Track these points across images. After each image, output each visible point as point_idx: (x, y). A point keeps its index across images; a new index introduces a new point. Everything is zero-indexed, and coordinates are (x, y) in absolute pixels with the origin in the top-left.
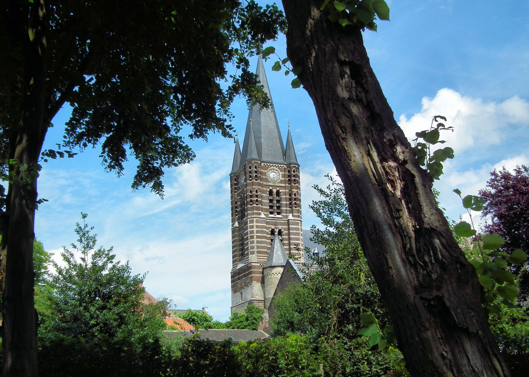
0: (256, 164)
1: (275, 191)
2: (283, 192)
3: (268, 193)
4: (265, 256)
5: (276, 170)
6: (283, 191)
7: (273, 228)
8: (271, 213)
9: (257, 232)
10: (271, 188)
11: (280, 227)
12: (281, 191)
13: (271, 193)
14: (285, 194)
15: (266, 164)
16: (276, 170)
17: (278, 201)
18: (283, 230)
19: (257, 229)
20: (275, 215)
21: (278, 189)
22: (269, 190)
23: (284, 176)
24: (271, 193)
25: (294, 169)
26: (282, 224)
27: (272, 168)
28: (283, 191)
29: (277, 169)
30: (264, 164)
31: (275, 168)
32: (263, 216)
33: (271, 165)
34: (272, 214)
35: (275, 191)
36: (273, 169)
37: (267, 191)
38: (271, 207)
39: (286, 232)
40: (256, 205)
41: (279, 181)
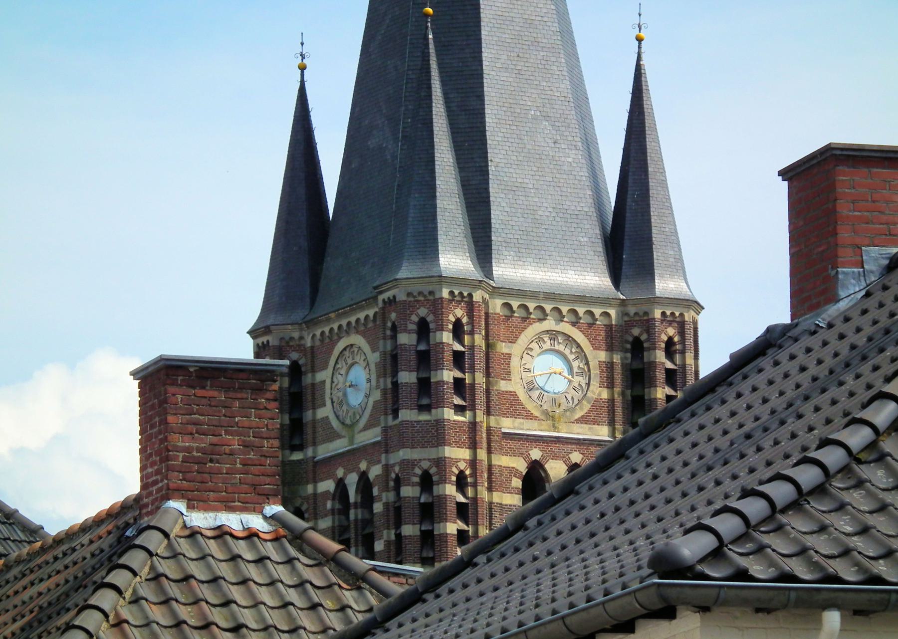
5: (568, 338)
22: (522, 466)
36: (553, 335)
37: (513, 471)
41: (587, 406)
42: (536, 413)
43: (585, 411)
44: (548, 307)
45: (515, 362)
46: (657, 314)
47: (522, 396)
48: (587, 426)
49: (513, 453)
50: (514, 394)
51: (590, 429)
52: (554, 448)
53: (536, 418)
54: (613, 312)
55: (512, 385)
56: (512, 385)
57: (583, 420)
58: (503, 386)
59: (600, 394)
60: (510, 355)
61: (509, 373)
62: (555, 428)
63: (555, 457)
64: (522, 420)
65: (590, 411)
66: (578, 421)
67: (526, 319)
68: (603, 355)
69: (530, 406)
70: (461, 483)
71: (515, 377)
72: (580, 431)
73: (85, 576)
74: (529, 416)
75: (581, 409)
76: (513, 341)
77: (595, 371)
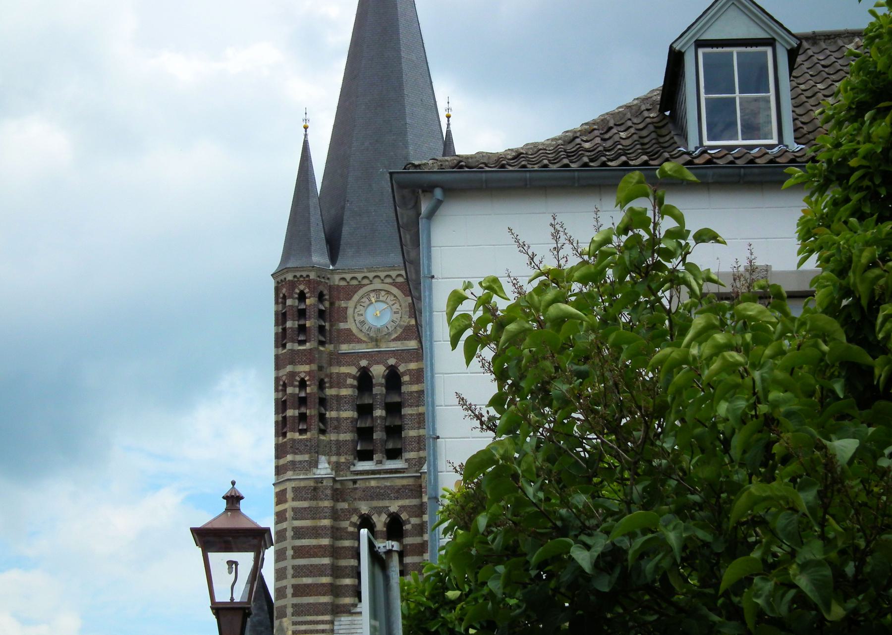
0: (302, 287)
1: (378, 371)
2: (409, 372)
3: (350, 381)
4: (323, 622)
5: (388, 292)
7: (364, 509)
8: (365, 456)
9: (299, 533)
10: (364, 363)
11: (394, 507)
12: (402, 368)
13: (364, 380)
15: (348, 277)
16: (388, 292)
18: (404, 516)
19: (298, 523)
20: (380, 462)
21: (392, 361)
22: (353, 370)
24: (364, 380)
26: (399, 492)
27: (377, 285)
29: (395, 291)
30: (343, 279)
32: (324, 469)
33: (371, 275)
34: (371, 459)
35: (378, 371)
37: (348, 375)
38: (364, 434)
39: (414, 521)
40: (297, 436)
41: (400, 331)
42: (364, 339)
43: (399, 333)
45: (350, 312)
48: (400, 342)
50: (349, 330)
51: (402, 343)
53: (364, 342)
55: (350, 325)
56: (350, 325)
58: (342, 326)
59: (409, 322)
60: (346, 308)
61: (346, 318)
62: (377, 346)
64: (354, 345)
65: (401, 333)
66: (394, 340)
67: (361, 286)
69: (361, 336)
72: (395, 345)
74: (359, 341)
75: (396, 332)
76: (349, 298)
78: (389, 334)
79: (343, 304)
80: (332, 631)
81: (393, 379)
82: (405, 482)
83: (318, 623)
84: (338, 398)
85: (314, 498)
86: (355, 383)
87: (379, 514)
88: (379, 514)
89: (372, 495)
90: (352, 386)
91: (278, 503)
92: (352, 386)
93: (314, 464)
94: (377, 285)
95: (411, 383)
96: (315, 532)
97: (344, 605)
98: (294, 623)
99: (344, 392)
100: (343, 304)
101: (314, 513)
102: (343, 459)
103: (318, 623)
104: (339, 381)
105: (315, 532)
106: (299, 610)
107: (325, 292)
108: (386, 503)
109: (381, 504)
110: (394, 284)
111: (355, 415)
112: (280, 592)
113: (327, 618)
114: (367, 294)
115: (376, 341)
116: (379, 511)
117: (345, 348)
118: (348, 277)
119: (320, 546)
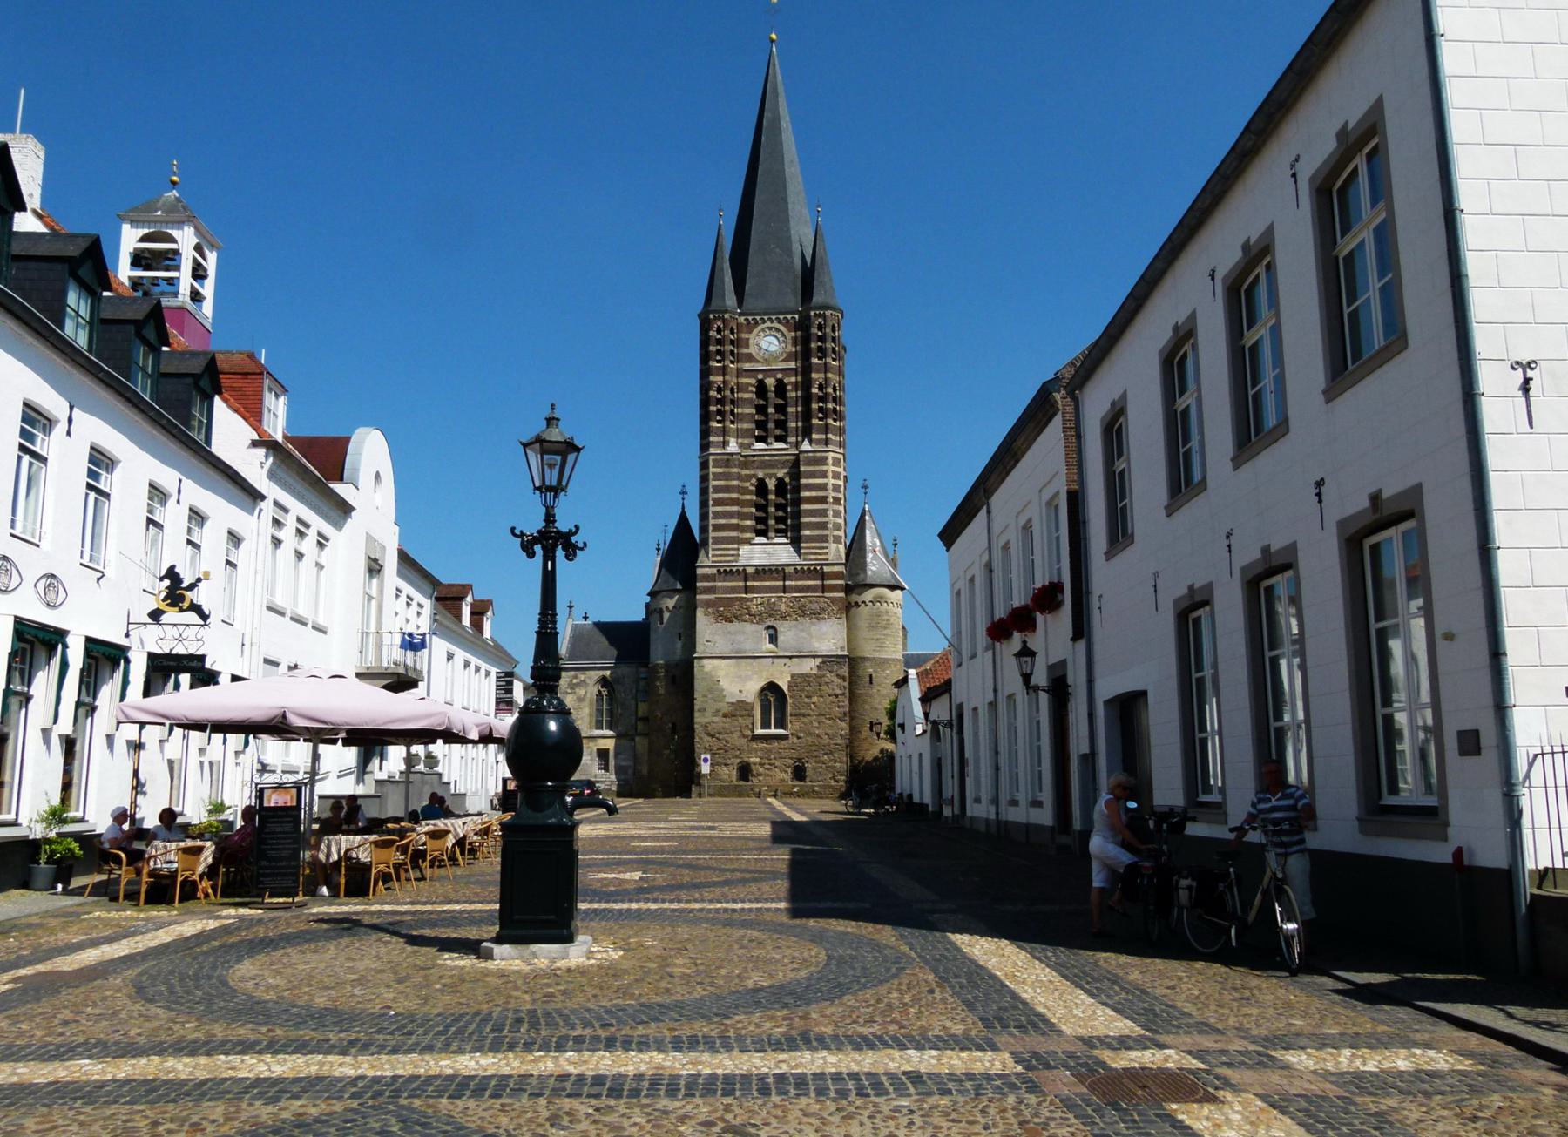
1: (770, 382)
2: (791, 383)
5: (777, 330)
6: (793, 379)
7: (760, 475)
10: (760, 376)
11: (781, 473)
12: (786, 381)
14: (796, 386)
15: (750, 318)
16: (777, 330)
17: (781, 409)
21: (779, 376)
22: (753, 381)
23: (795, 344)
24: (761, 389)
25: (820, 320)
27: (768, 324)
28: (793, 379)
29: (782, 328)
31: (776, 325)
32: (733, 446)
35: (770, 382)
36: (770, 328)
38: (761, 425)
41: (785, 355)
44: (766, 318)
45: (751, 341)
46: (812, 313)
47: (754, 354)
49: (749, 377)
50: (751, 354)
52: (769, 373)
54: (797, 316)
55: (752, 350)
57: (783, 361)
58: (745, 351)
63: (769, 376)
67: (757, 323)
68: (793, 334)
70: (719, 390)
71: (751, 347)
73: (1054, 504)
74: (757, 361)
76: (751, 332)
77: (789, 341)
78: (777, 357)
79: (744, 336)
80: (738, 555)
81: (781, 388)
82: (788, 457)
83: (729, 549)
84: (743, 400)
85: (727, 466)
86: (754, 390)
87: (770, 478)
88: (770, 478)
89: (764, 465)
90: (752, 392)
91: (701, 469)
92: (752, 392)
93: (725, 444)
94: (768, 324)
95: (792, 391)
96: (727, 489)
97: (746, 539)
98: (713, 550)
99: (746, 396)
100: (744, 336)
101: (727, 477)
102: (746, 441)
103: (729, 549)
104: (741, 388)
105: (727, 489)
106: (717, 541)
107: (735, 327)
108: (775, 471)
109: (771, 471)
110: (780, 322)
111: (754, 411)
112: (704, 529)
113: (736, 546)
114: (763, 330)
115: (766, 361)
116: (770, 476)
117: (747, 366)
118: (750, 318)
119: (731, 499)
